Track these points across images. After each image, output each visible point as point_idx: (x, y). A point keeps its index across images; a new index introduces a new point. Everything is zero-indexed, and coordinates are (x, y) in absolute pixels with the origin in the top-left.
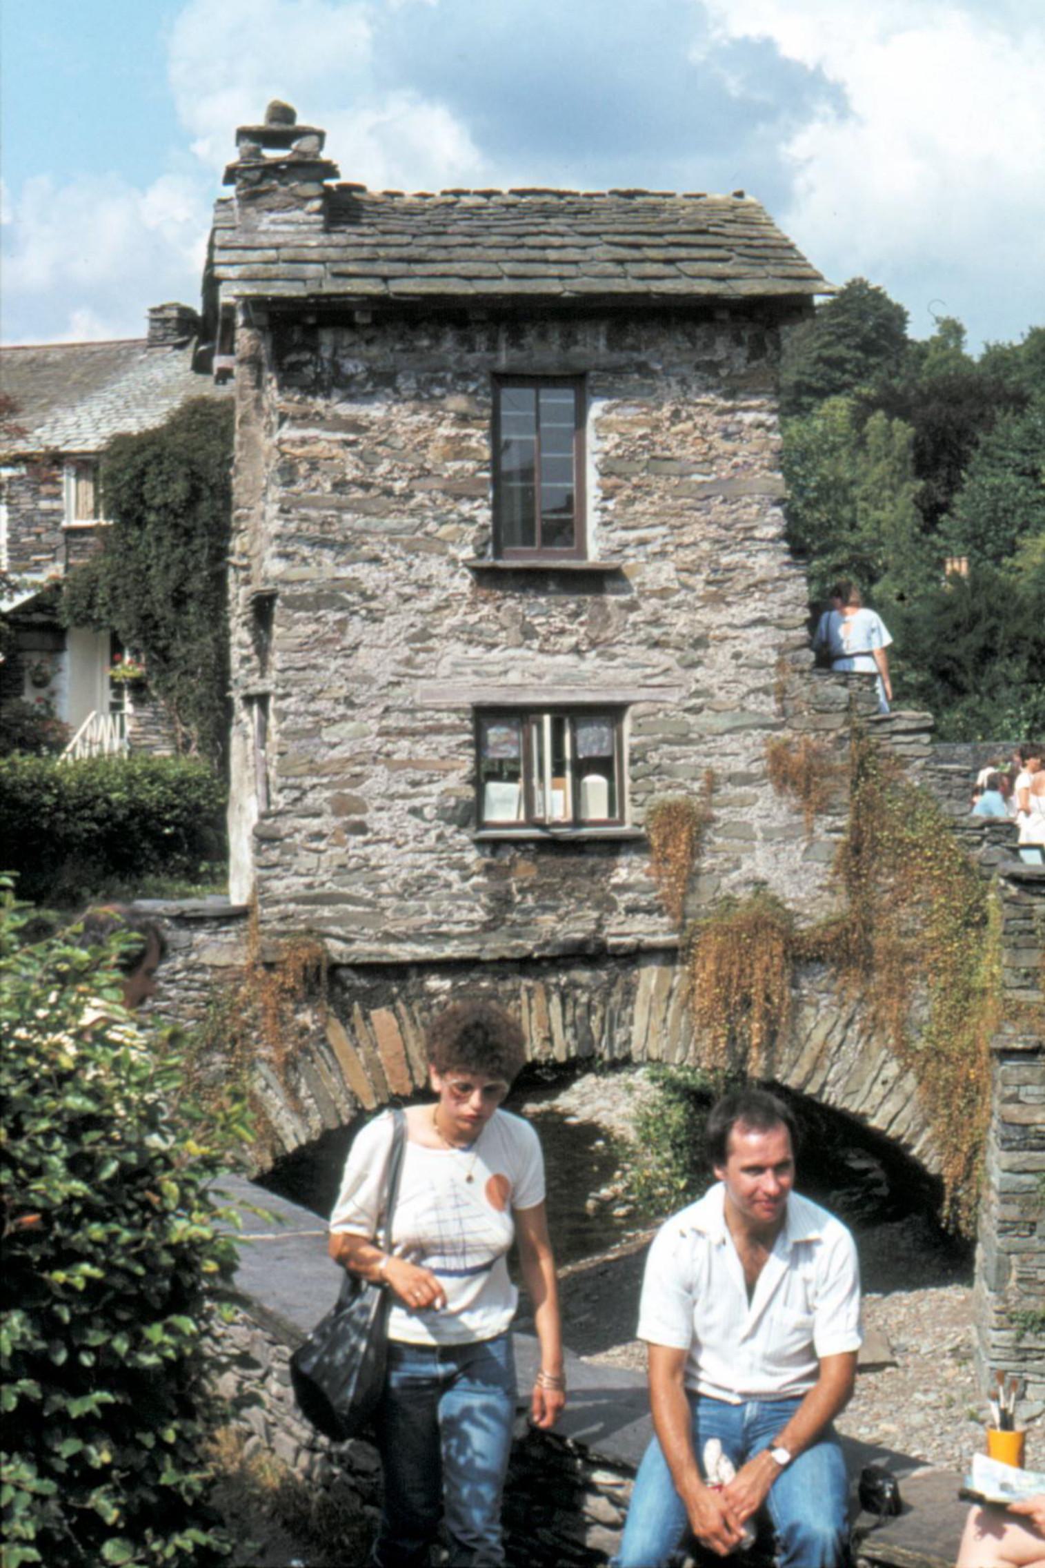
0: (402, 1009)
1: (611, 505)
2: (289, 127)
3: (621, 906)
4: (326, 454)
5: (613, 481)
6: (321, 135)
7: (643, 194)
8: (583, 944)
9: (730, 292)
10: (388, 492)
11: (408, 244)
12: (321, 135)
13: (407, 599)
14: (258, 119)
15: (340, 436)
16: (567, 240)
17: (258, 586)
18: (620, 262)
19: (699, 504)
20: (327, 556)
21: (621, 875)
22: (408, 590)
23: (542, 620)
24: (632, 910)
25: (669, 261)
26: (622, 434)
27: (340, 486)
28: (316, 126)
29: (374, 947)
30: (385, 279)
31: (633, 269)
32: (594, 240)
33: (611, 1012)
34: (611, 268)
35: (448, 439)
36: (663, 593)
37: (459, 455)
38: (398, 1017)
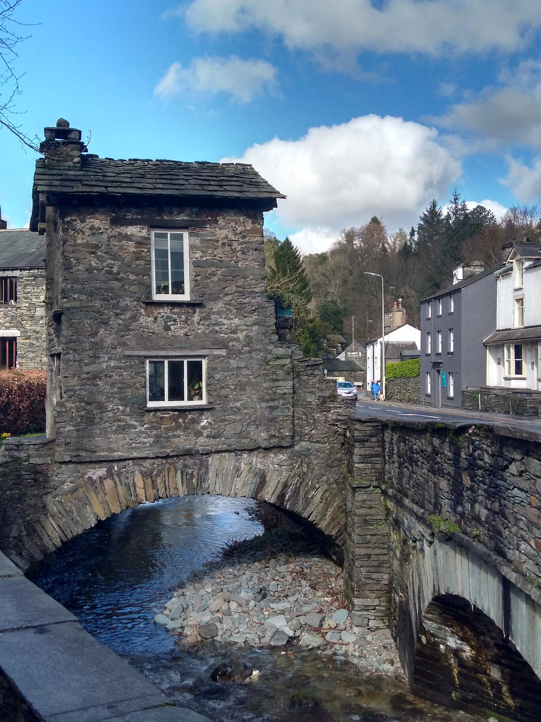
0: (117, 478)
1: (198, 278)
2: (67, 128)
3: (205, 435)
4: (83, 257)
5: (198, 269)
6: (80, 132)
7: (209, 163)
8: (190, 450)
9: (245, 196)
10: (110, 272)
11: (116, 176)
12: (80, 132)
13: (117, 315)
14: (54, 125)
15: (89, 250)
16: (179, 177)
17: (56, 309)
18: (200, 185)
19: (233, 279)
20: (83, 297)
21: (204, 423)
22: (118, 311)
23: (172, 323)
24: (208, 437)
25: (221, 186)
26: (203, 252)
27: (90, 270)
28: (78, 129)
29: (106, 453)
30: (106, 187)
31: (205, 187)
32: (189, 178)
33: (201, 477)
34: (198, 187)
35: (133, 252)
36: (219, 313)
37: (138, 259)
38: (115, 482)
